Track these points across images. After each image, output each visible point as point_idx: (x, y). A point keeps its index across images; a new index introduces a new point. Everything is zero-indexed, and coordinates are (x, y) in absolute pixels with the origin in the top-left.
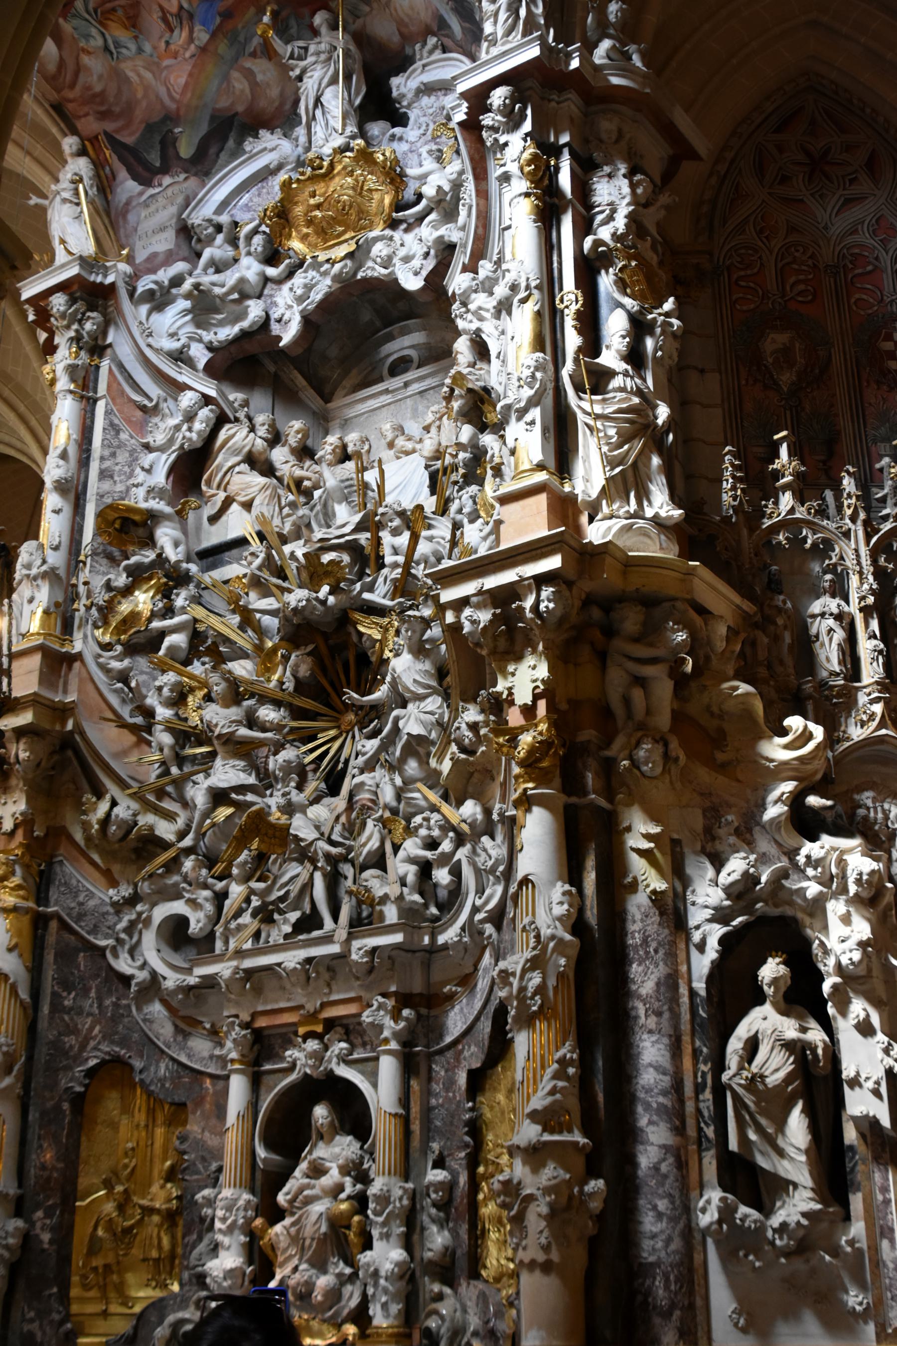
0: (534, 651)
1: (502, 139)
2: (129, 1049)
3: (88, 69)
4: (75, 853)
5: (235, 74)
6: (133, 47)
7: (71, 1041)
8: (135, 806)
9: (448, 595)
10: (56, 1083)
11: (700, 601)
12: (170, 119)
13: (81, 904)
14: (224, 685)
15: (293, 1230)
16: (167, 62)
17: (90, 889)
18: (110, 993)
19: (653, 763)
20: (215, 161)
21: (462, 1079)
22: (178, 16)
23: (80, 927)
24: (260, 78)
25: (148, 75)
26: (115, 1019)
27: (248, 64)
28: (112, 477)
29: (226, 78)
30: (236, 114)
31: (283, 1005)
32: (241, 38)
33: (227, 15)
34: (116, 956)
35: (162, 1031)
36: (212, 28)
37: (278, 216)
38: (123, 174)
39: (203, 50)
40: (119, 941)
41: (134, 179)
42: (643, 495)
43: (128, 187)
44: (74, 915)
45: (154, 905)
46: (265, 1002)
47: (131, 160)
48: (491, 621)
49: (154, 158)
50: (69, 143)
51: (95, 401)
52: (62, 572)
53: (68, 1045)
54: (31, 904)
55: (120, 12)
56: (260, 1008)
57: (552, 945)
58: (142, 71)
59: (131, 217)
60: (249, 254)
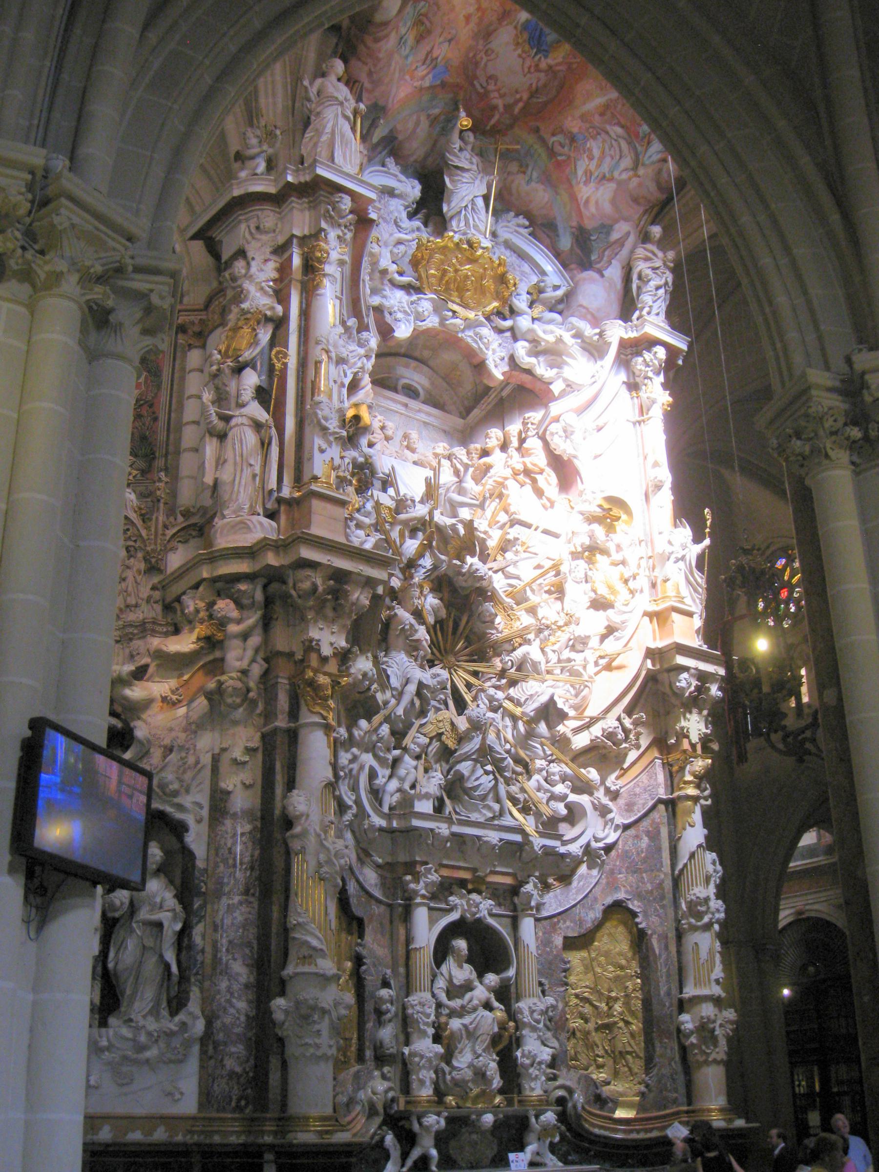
0: (700, 713)
1: (650, 374)
9: (681, 660)
15: (471, 1027)
16: (407, 77)
21: (559, 941)
24: (418, 130)
25: (397, 75)
27: (423, 118)
30: (396, 138)
31: (462, 864)
36: (434, 84)
39: (421, 89)
46: (448, 858)
55: (422, 28)
56: (445, 862)
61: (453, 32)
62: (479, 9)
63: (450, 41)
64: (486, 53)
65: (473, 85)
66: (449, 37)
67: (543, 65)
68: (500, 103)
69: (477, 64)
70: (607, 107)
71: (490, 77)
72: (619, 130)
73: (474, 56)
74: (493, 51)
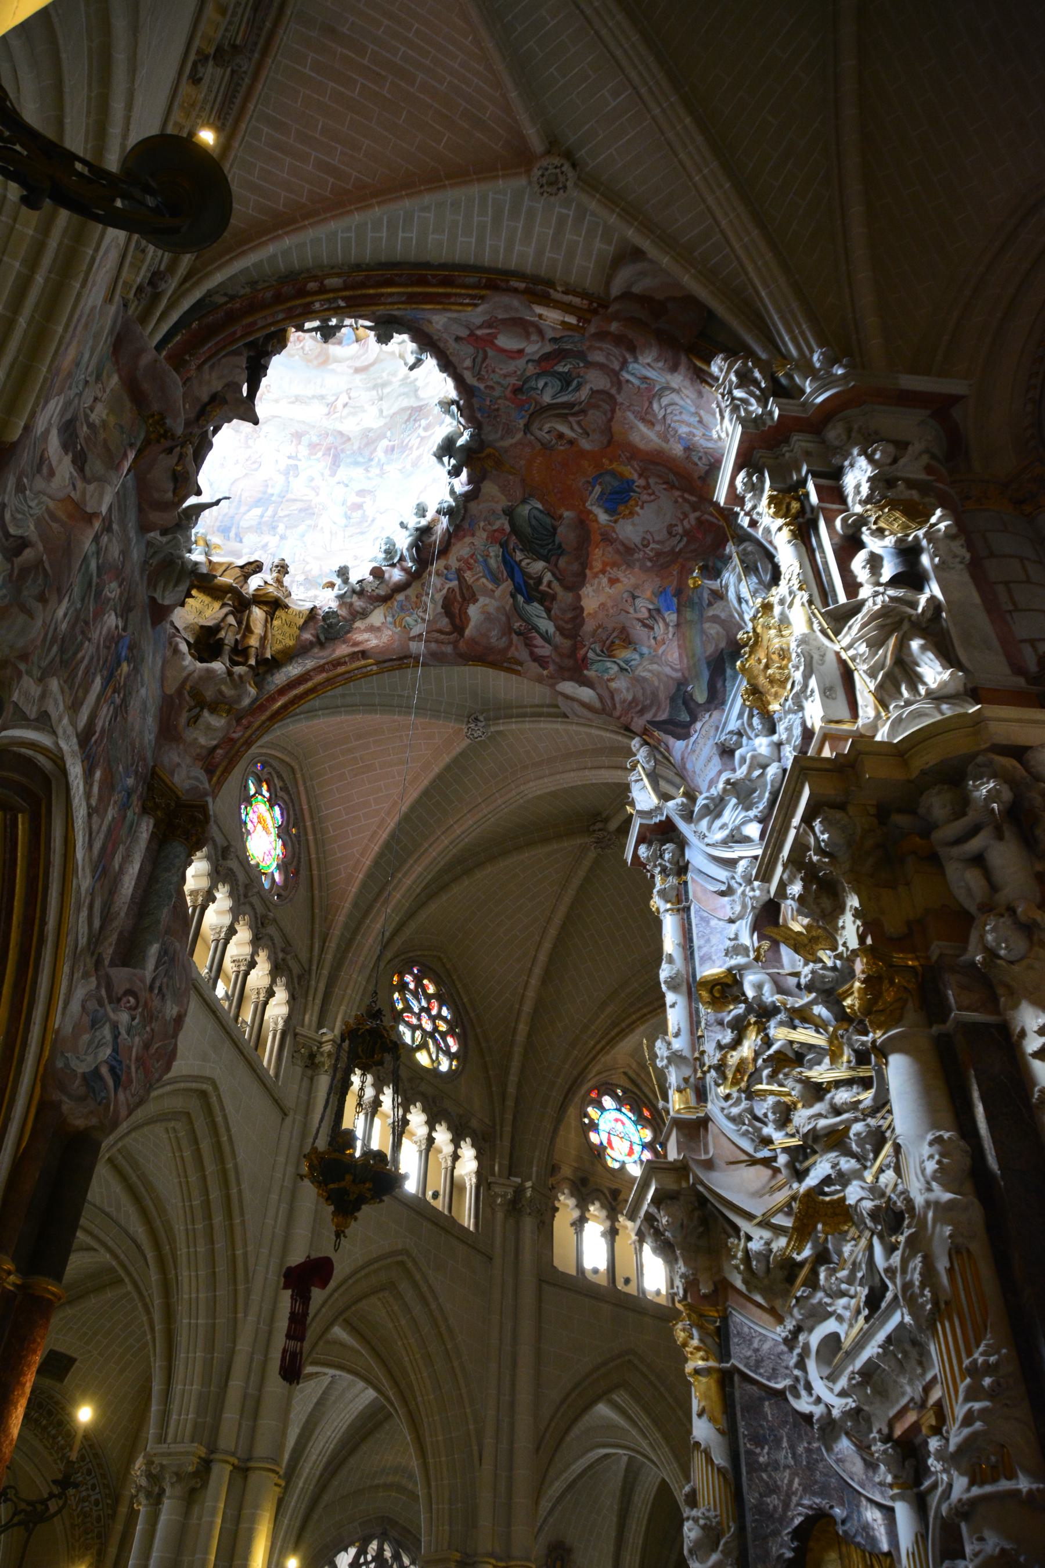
2: (829, 1496)
3: (617, 690)
4: (742, 1300)
5: (706, 625)
6: (637, 657)
7: (773, 1501)
8: (767, 1234)
10: (767, 1552)
11: (1005, 742)
12: (681, 684)
13: (756, 1350)
14: (799, 1086)
17: (760, 1332)
18: (800, 1438)
19: (1006, 941)
20: (725, 691)
22: (651, 616)
23: (760, 1375)
24: (723, 616)
25: (655, 667)
26: (811, 1467)
27: (711, 613)
28: (710, 958)
29: (703, 632)
32: (696, 600)
33: (679, 593)
34: (797, 1396)
35: (854, 1470)
36: (675, 607)
37: (753, 694)
38: (671, 741)
39: (678, 625)
40: (797, 1379)
41: (679, 737)
42: (915, 680)
43: (678, 746)
44: (752, 1363)
45: (811, 1330)
47: (671, 728)
48: (804, 887)
49: (685, 717)
50: (635, 743)
51: (689, 908)
52: (686, 1053)
53: (771, 1507)
54: (711, 1363)
55: (617, 642)
56: (892, 1413)
57: (930, 1215)
58: (650, 667)
59: (689, 766)
60: (757, 736)
61: (625, 595)
62: (603, 572)
63: (634, 597)
64: (646, 546)
65: (680, 551)
66: (630, 600)
67: (641, 482)
68: (693, 516)
69: (659, 554)
70: (643, 420)
71: (670, 533)
72: (655, 406)
73: (650, 560)
74: (644, 539)
